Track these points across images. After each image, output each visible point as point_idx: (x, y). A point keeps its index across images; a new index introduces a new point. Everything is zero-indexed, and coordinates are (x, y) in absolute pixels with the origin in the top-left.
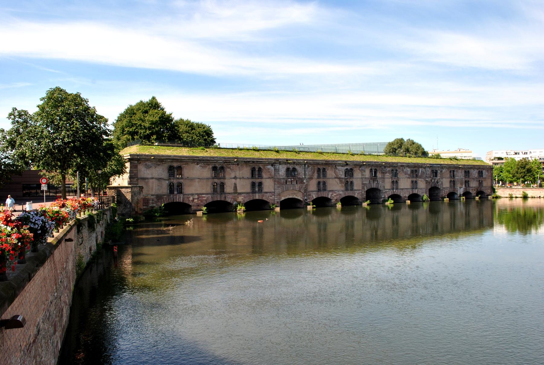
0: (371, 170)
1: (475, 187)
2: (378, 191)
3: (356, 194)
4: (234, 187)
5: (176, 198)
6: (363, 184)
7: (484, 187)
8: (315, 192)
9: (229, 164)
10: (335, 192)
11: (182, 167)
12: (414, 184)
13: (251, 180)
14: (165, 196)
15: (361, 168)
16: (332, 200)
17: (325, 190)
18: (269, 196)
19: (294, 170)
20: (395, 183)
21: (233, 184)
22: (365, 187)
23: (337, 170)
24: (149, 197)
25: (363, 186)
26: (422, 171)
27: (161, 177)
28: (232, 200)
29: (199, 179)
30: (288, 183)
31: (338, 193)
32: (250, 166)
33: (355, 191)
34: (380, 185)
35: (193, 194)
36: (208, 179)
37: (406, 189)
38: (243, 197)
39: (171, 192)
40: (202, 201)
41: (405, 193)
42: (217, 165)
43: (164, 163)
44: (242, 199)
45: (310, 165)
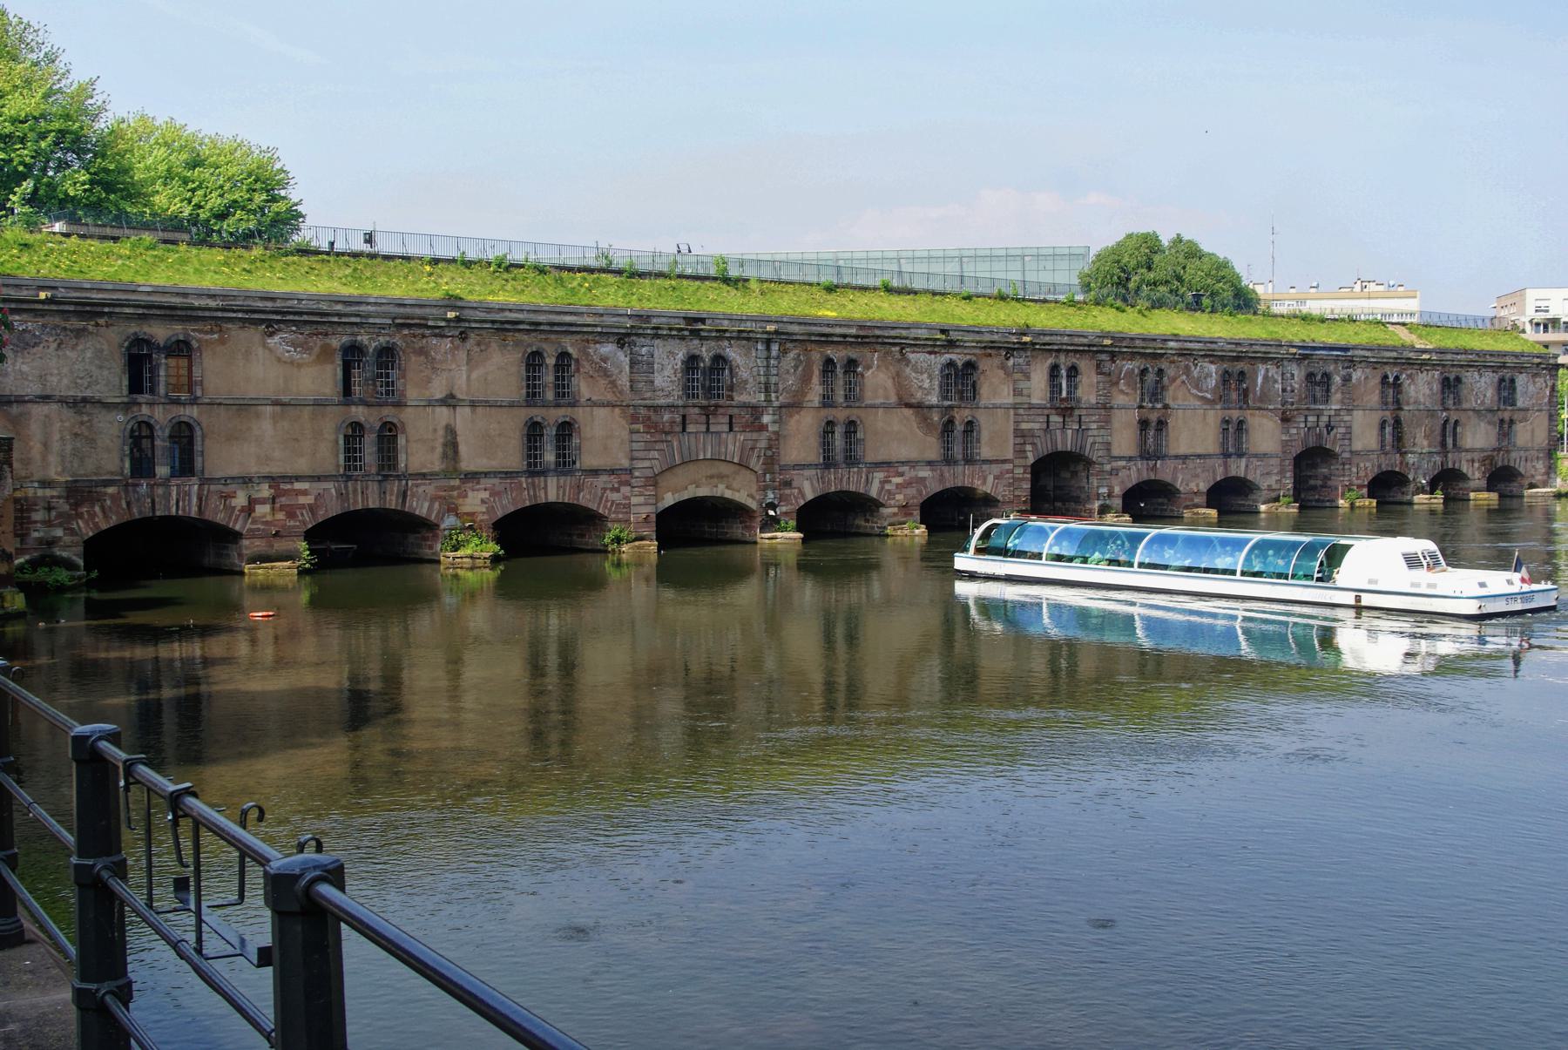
0: (1054, 371)
1: (1482, 450)
2: (1080, 467)
3: (990, 478)
4: (445, 445)
5: (167, 496)
6: (1019, 433)
7: (1521, 449)
8: (813, 472)
9: (420, 331)
10: (901, 469)
11: (195, 344)
12: (1234, 434)
13: (524, 414)
14: (110, 490)
15: (1011, 362)
16: (883, 505)
17: (851, 460)
18: (605, 489)
19: (719, 360)
20: (1152, 428)
21: (441, 432)
22: (1029, 448)
23: (908, 370)
24: (30, 492)
25: (1019, 440)
26: (1266, 378)
27: (88, 393)
28: (437, 505)
29: (276, 403)
30: (691, 428)
31: (913, 474)
32: (517, 343)
33: (985, 467)
34: (1090, 440)
35: (250, 480)
36: (318, 404)
37: (1199, 456)
38: (485, 495)
39: (142, 466)
41: (1197, 476)
42: (363, 338)
43: (101, 321)
44: (483, 501)
45: (789, 345)
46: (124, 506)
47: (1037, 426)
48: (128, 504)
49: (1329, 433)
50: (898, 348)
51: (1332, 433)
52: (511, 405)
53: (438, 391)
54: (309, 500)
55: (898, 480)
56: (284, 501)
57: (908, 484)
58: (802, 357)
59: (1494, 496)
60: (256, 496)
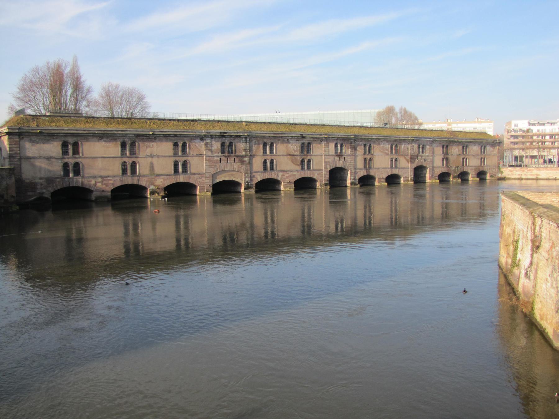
1: (475, 166)
3: (316, 175)
6: (325, 162)
10: (288, 172)
12: (394, 162)
13: (173, 159)
14: (58, 180)
22: (328, 166)
32: (171, 140)
34: (348, 164)
37: (383, 168)
38: (162, 180)
40: (107, 185)
41: (382, 174)
43: (55, 137)
45: (253, 139)
46: (62, 183)
47: (331, 160)
48: (63, 183)
49: (425, 161)
50: (286, 139)
51: (426, 162)
52: (169, 157)
53: (148, 152)
54: (112, 182)
55: (287, 175)
56: (105, 182)
57: (291, 176)
58: (257, 142)
59: (478, 179)
60: (97, 181)
